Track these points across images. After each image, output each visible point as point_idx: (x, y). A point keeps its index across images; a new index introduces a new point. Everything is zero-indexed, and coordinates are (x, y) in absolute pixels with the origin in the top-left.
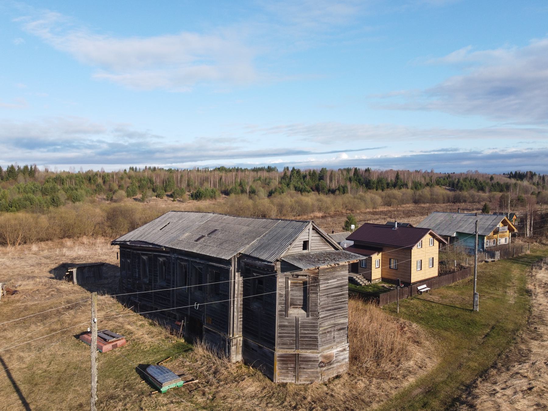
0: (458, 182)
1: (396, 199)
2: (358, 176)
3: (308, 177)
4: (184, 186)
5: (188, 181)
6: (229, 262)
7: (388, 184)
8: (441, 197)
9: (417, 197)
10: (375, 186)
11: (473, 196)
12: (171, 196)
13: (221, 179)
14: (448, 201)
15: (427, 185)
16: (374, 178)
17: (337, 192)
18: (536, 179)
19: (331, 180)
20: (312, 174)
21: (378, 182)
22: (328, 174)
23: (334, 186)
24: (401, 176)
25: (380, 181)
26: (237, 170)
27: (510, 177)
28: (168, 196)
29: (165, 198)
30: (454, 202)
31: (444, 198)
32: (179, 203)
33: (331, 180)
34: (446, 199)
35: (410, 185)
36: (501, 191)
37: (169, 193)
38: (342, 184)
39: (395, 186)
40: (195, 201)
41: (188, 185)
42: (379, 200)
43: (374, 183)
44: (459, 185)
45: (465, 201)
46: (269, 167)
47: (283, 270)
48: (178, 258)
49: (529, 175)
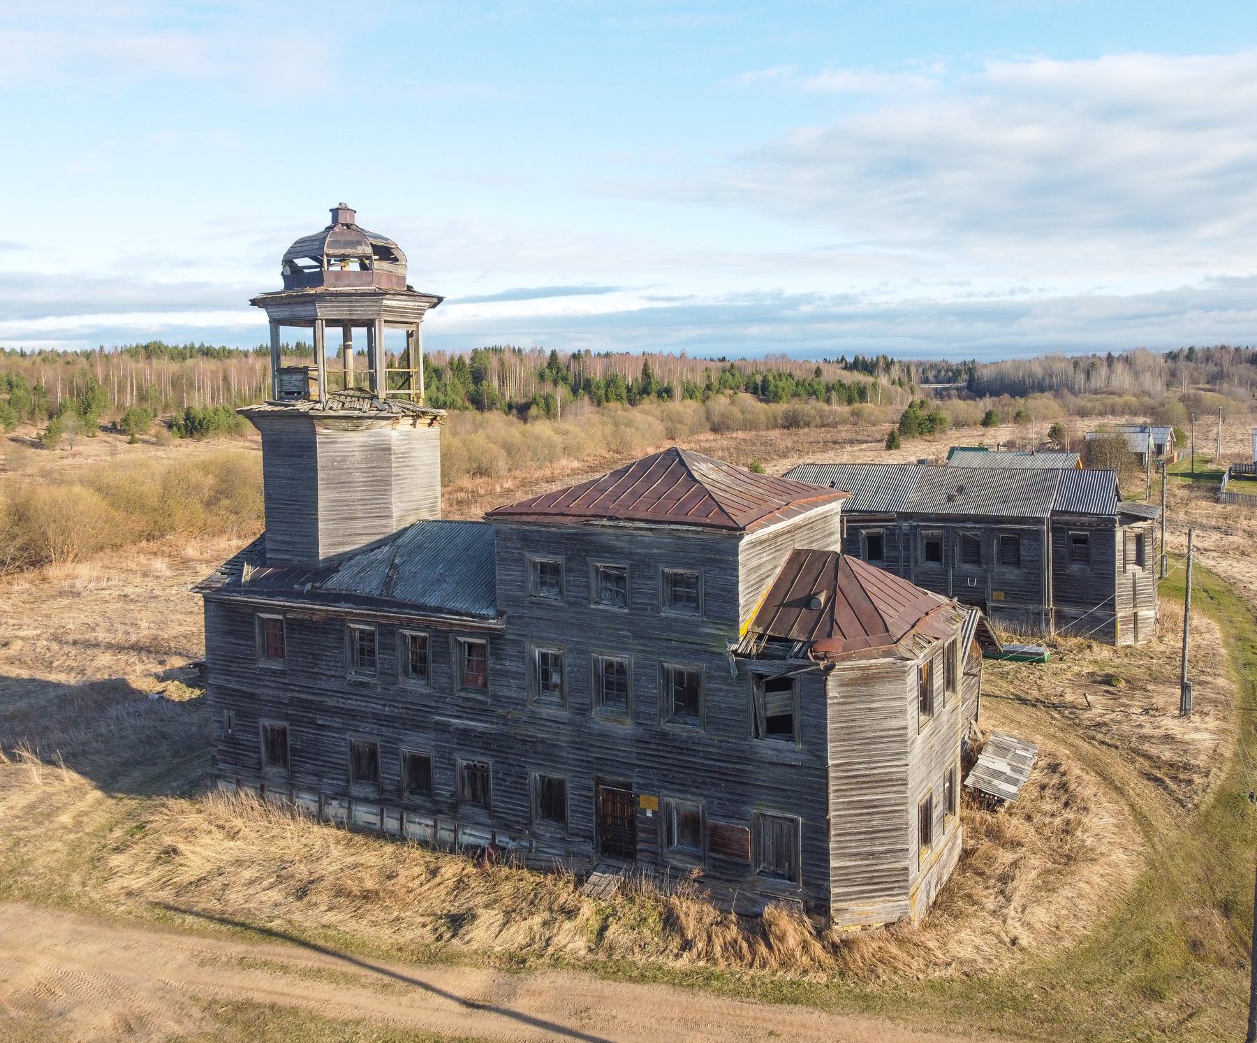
0: (765, 380)
1: (681, 422)
2: (559, 370)
3: (449, 373)
4: (130, 400)
5: (140, 389)
6: (1039, 521)
7: (629, 390)
8: (762, 417)
9: (716, 419)
10: (602, 392)
11: (820, 413)
12: (112, 429)
13: (225, 379)
14: (775, 426)
15: (708, 388)
16: (597, 373)
17: (534, 411)
18: (895, 372)
19: (503, 379)
20: (457, 366)
21: (608, 385)
22: (494, 363)
23: (512, 392)
24: (656, 371)
25: (611, 382)
26: (207, 352)
27: (845, 368)
28: (105, 429)
29: (101, 435)
30: (787, 427)
31: (767, 418)
32: (152, 448)
33: (503, 379)
34: (772, 419)
35: (678, 391)
36: (850, 401)
37: (105, 422)
38: (533, 389)
39: (645, 391)
40: (189, 440)
41: (142, 398)
42: (659, 428)
43: (598, 387)
44: (772, 388)
45: (807, 424)
46: (298, 345)
47: (1121, 524)
48: (915, 527)
49: (881, 364)
